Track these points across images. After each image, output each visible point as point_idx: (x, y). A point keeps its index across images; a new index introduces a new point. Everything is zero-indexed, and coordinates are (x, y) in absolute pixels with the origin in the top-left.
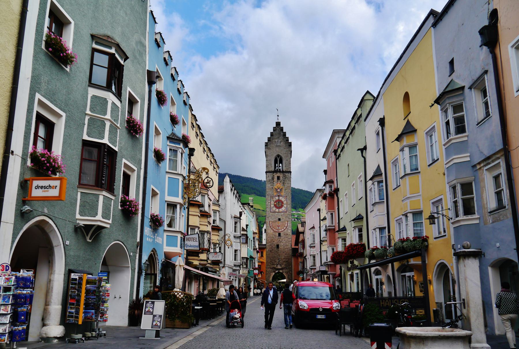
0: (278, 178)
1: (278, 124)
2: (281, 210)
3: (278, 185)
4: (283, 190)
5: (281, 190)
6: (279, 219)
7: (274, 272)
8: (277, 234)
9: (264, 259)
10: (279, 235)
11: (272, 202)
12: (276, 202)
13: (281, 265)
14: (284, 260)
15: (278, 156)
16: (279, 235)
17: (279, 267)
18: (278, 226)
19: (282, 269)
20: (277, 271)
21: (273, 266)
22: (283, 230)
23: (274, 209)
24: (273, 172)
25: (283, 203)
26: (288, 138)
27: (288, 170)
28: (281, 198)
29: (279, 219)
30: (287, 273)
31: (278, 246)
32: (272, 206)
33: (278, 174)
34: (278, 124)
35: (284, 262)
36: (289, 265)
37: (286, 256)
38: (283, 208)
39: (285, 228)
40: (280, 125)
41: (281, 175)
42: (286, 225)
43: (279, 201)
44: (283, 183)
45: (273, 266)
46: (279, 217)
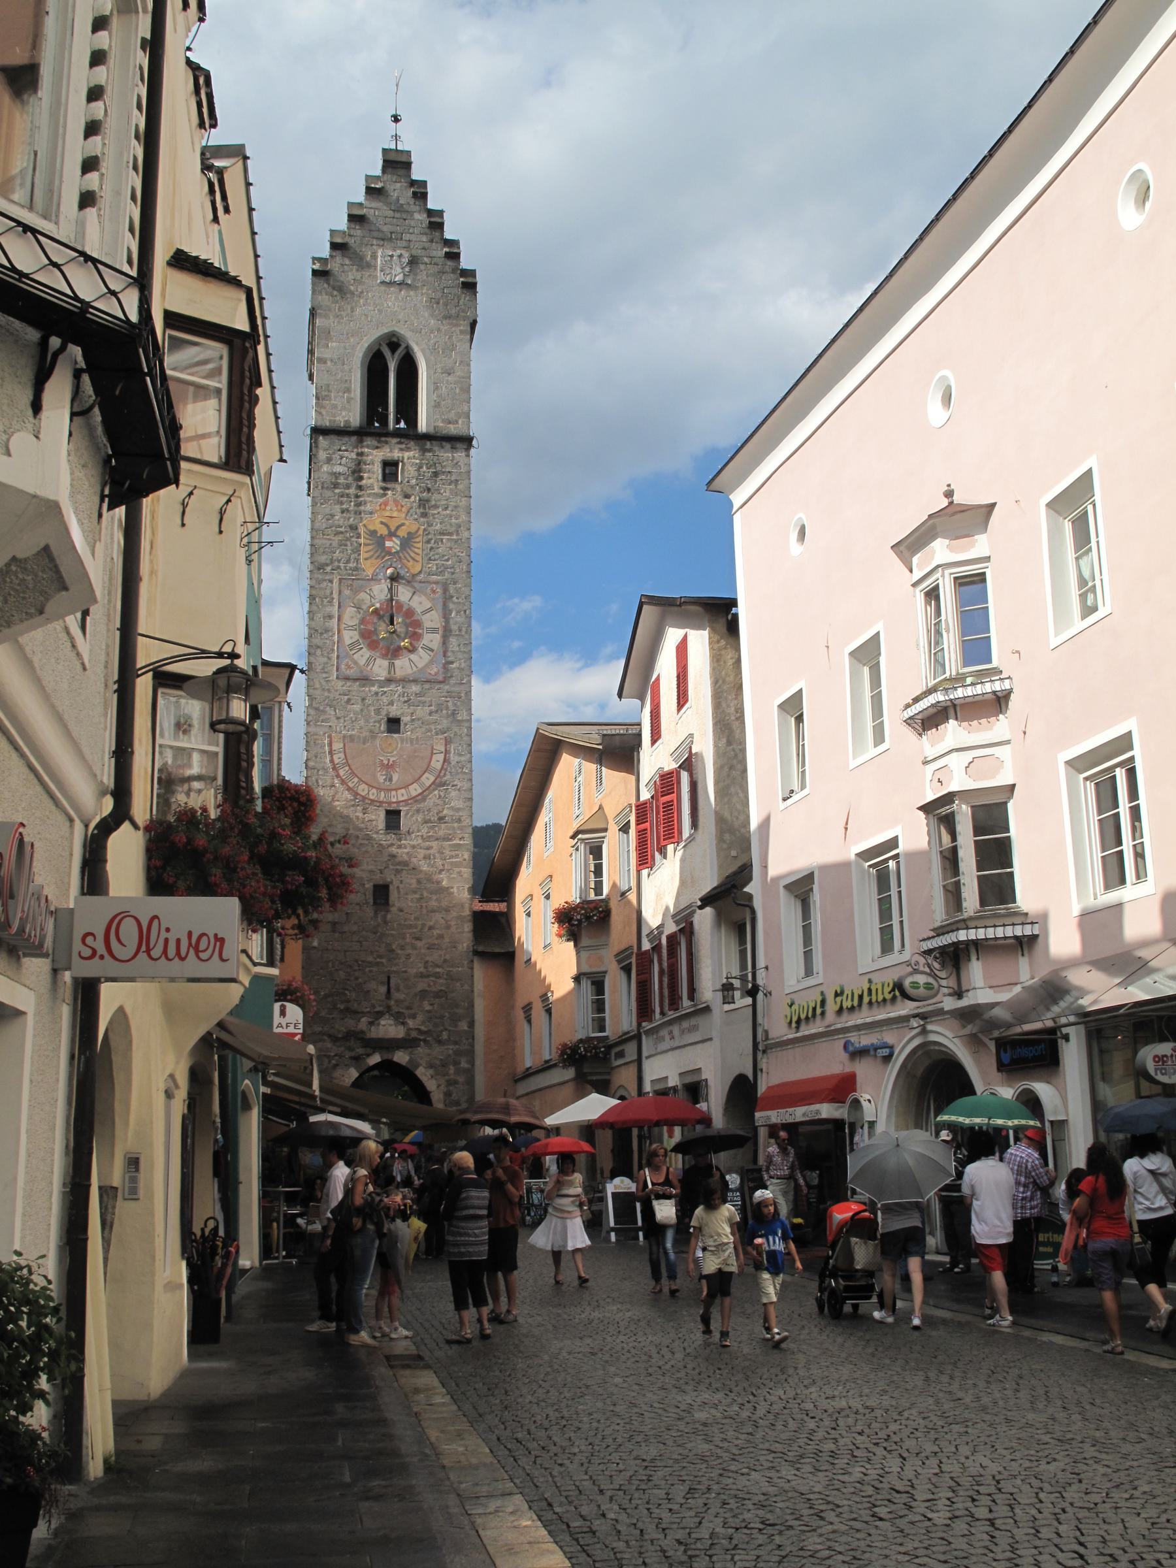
0: (390, 469)
2: (404, 666)
3: (391, 511)
5: (407, 543)
6: (394, 724)
7: (357, 1059)
8: (379, 819)
10: (393, 817)
11: (351, 616)
13: (399, 1018)
14: (422, 985)
15: (394, 342)
16: (393, 817)
17: (388, 1029)
18: (389, 767)
19: (407, 1043)
20: (375, 1059)
21: (350, 1023)
22: (415, 790)
23: (363, 655)
24: (360, 433)
25: (418, 624)
26: (453, 243)
27: (453, 430)
28: (403, 594)
29: (394, 724)
30: (439, 1067)
32: (350, 637)
33: (391, 451)
34: (396, 163)
35: (423, 994)
36: (455, 1020)
37: (435, 956)
38: (421, 658)
39: (428, 779)
40: (407, 165)
41: (409, 457)
42: (437, 762)
44: (423, 503)
45: (350, 1023)
46: (394, 711)
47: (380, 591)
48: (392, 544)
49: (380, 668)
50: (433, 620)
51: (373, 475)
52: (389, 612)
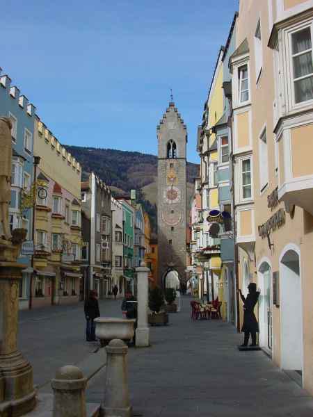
0: (171, 164)
1: (171, 105)
2: (174, 201)
4: (177, 179)
5: (175, 178)
6: (172, 212)
9: (155, 256)
10: (172, 228)
11: (165, 193)
12: (169, 192)
16: (172, 228)
18: (172, 220)
24: (166, 159)
27: (182, 157)
28: (174, 188)
31: (170, 241)
34: (171, 105)
40: (173, 106)
43: (172, 191)
47: (170, 188)
48: (172, 179)
49: (170, 202)
50: (179, 193)
51: (168, 167)
52: (172, 191)
